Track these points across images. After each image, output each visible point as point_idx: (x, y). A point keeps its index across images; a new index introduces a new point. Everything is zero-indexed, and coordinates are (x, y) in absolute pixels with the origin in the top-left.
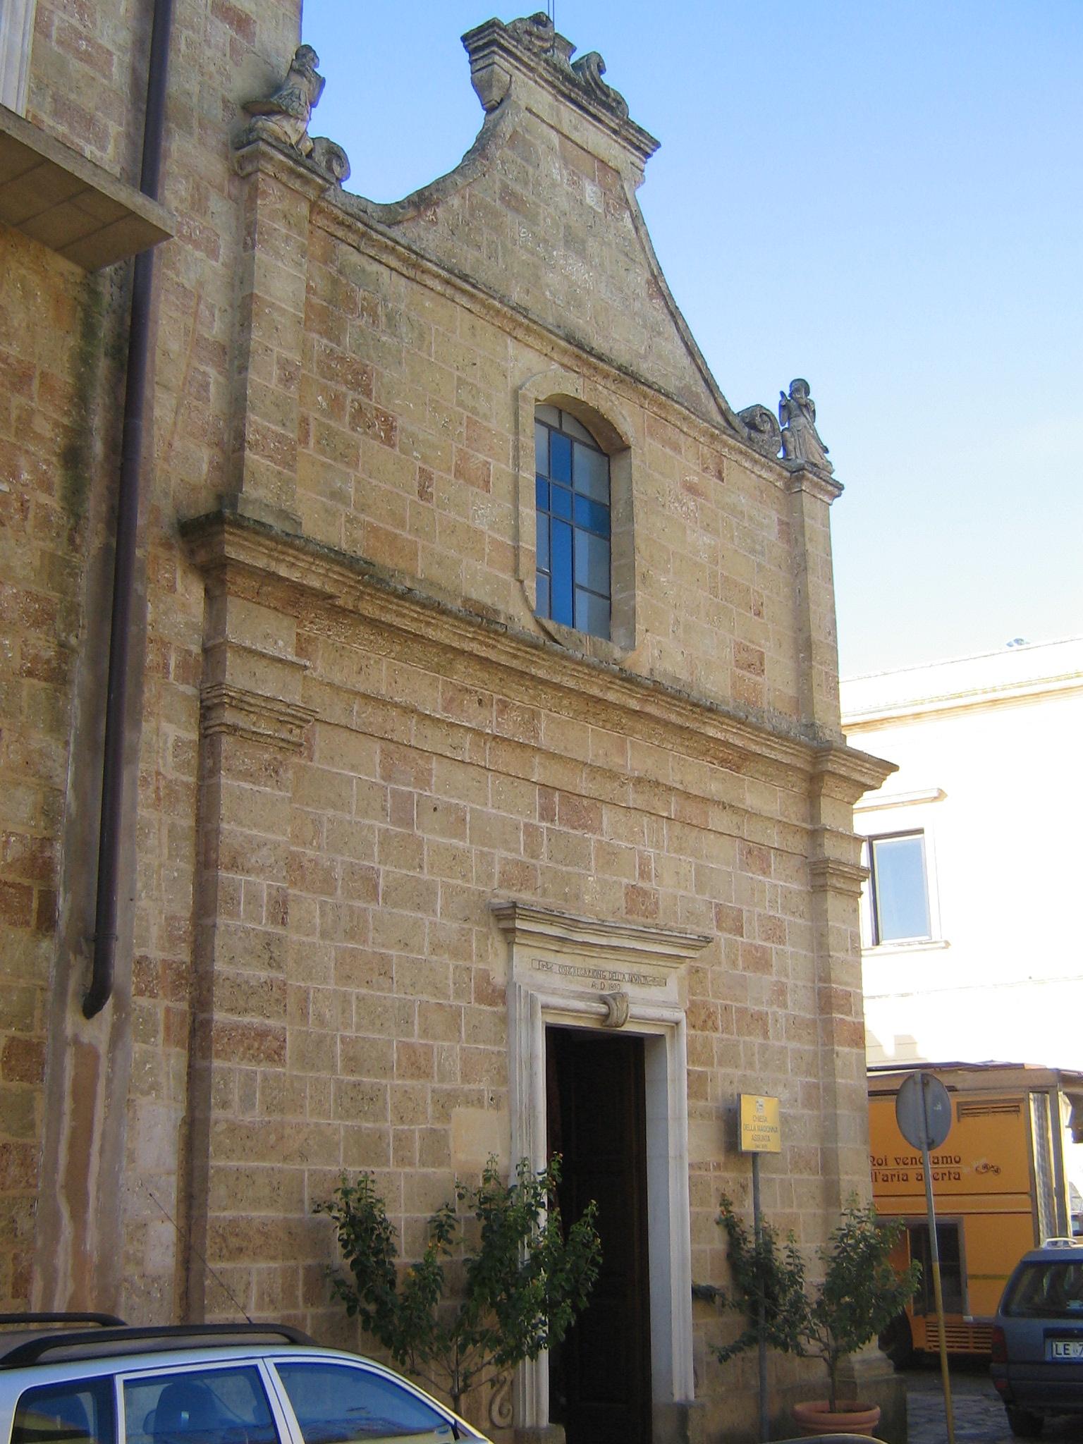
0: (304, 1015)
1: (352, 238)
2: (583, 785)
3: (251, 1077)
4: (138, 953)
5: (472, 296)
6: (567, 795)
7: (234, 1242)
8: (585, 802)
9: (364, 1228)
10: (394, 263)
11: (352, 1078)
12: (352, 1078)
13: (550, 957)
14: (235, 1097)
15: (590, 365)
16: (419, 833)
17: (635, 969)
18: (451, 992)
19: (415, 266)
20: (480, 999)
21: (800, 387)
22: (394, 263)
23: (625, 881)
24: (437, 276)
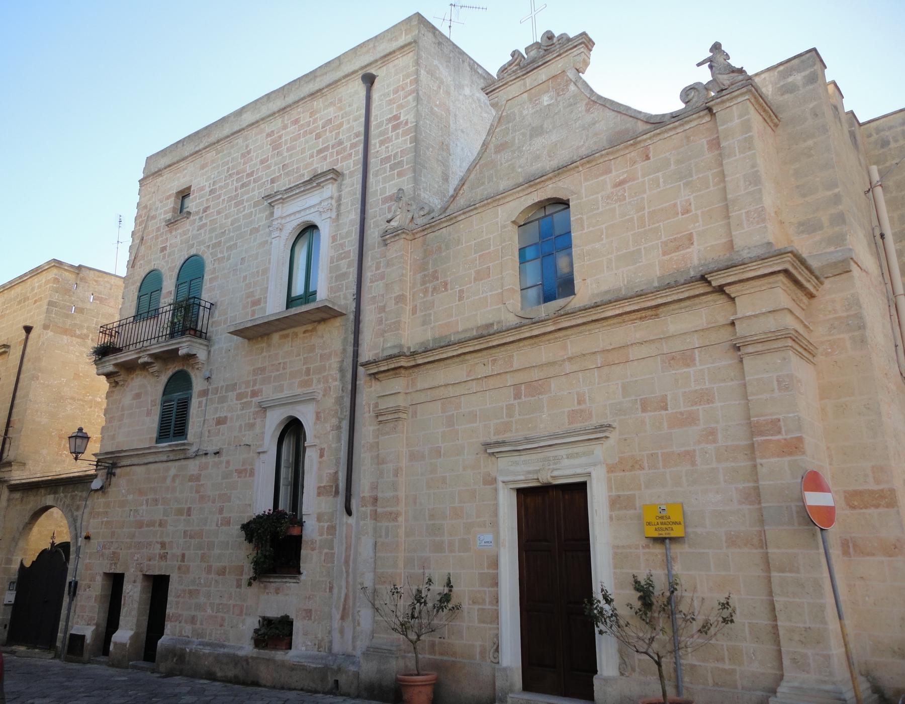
0: (415, 503)
1: (429, 231)
2: (536, 375)
3: (387, 527)
4: (362, 495)
5: (476, 209)
6: (528, 384)
7: (383, 579)
8: (540, 382)
9: (637, 582)
10: (445, 225)
11: (432, 522)
12: (432, 522)
13: (517, 458)
14: (383, 534)
15: (539, 183)
16: (456, 427)
17: (570, 451)
18: (646, 467)
19: (451, 219)
20: (484, 484)
21: (716, 47)
22: (445, 225)
23: (566, 410)
24: (460, 215)
